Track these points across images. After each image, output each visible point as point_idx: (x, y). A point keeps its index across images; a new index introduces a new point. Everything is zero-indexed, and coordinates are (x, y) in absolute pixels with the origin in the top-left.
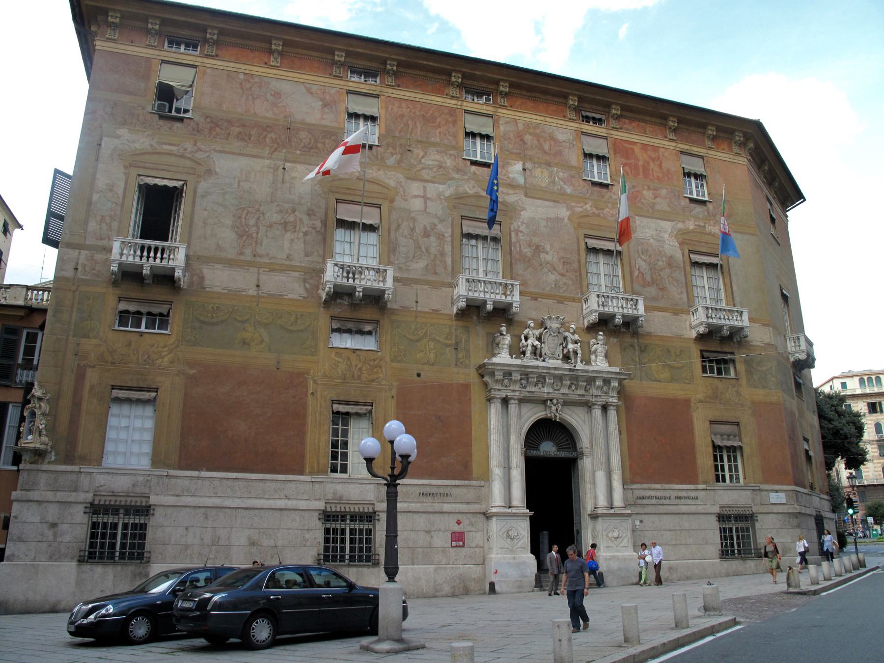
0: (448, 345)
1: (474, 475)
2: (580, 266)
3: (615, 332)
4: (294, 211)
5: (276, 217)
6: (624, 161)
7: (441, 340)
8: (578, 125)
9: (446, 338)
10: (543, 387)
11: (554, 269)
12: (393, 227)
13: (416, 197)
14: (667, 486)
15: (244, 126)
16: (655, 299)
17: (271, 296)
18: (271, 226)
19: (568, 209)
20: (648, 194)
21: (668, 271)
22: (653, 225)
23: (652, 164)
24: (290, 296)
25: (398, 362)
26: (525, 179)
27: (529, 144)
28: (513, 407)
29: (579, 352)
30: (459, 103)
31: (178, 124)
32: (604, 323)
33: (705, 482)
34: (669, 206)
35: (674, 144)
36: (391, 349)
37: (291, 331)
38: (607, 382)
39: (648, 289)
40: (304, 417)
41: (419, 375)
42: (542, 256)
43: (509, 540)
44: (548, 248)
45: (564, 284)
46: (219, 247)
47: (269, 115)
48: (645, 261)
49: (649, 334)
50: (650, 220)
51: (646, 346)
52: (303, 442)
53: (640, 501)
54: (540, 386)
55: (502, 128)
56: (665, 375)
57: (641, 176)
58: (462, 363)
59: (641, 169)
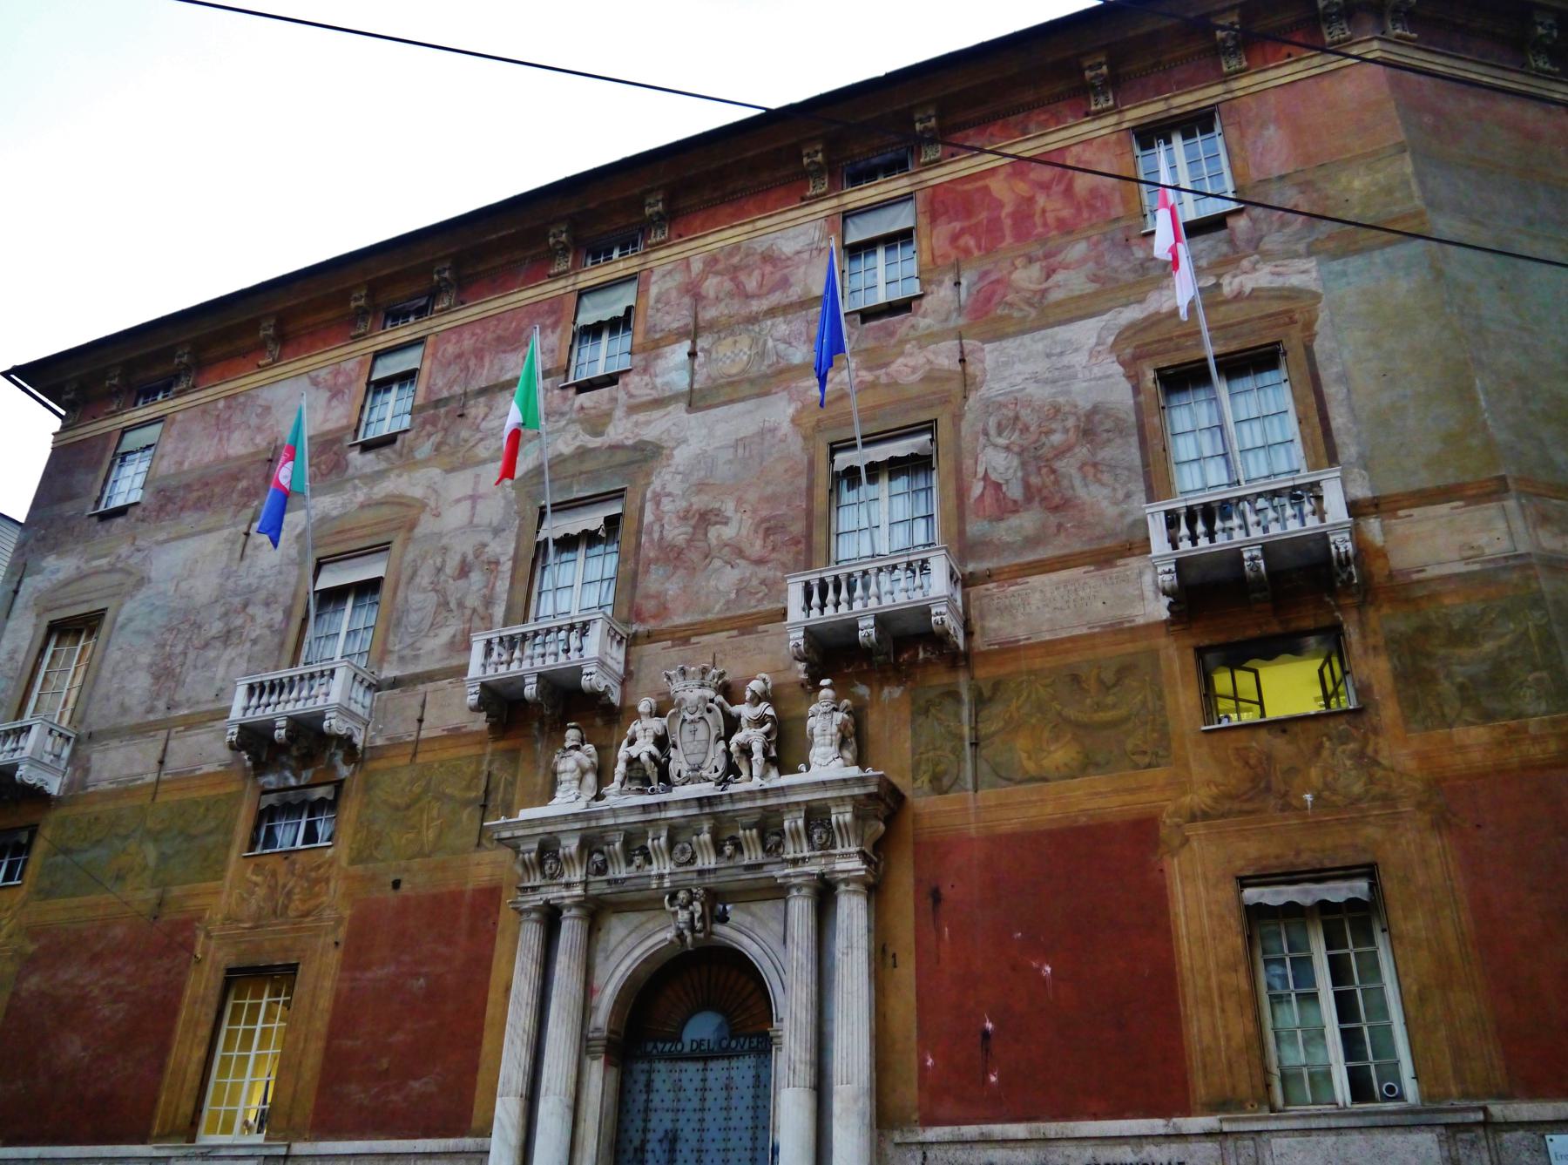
2: (810, 527)
3: (896, 667)
4: (245, 606)
5: (216, 627)
6: (957, 225)
7: (457, 793)
8: (834, 202)
9: (468, 788)
10: (651, 863)
11: (740, 553)
12: (404, 579)
13: (458, 501)
14: (1052, 1128)
15: (207, 484)
16: (1033, 542)
17: (178, 776)
18: (206, 645)
19: (791, 400)
20: (1026, 277)
21: (1082, 452)
22: (1040, 346)
23: (1041, 200)
24: (206, 769)
25: (361, 861)
26: (693, 373)
27: (712, 294)
28: (571, 931)
29: (757, 747)
30: (571, 281)
31: (120, 520)
32: (832, 654)
33: (1217, 1106)
34: (1095, 279)
35: (1113, 120)
36: (355, 834)
37: (195, 837)
38: (816, 816)
39: (1014, 521)
40: (174, 1013)
41: (396, 884)
42: (713, 532)
44: (729, 508)
45: (763, 582)
46: (124, 709)
47: (251, 449)
48: (1007, 448)
49: (1010, 649)
50: (1027, 338)
51: (997, 685)
52: (160, 1068)
54: (638, 860)
55: (654, 291)
56: (1061, 755)
57: (1009, 240)
59: (1008, 222)
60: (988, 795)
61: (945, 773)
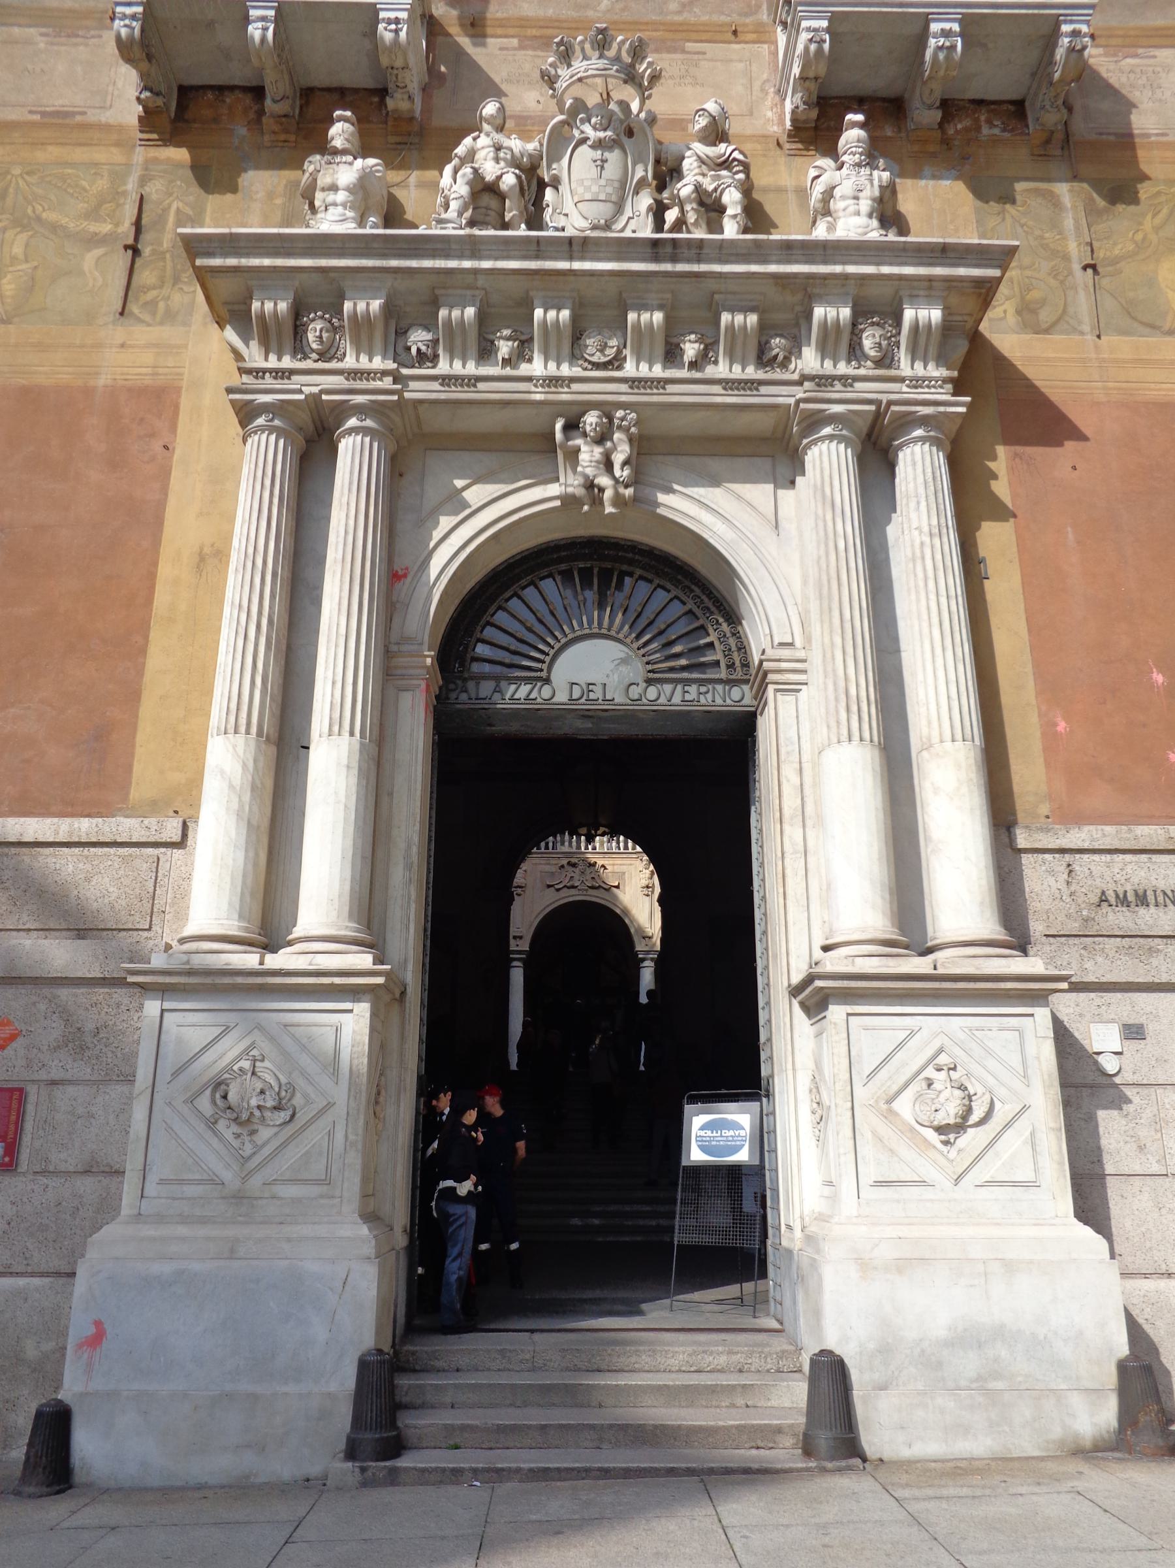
0: (94, 241)
1: (134, 794)
9: (93, 214)
29: (732, 198)
43: (226, 1129)
53: (1118, 919)
58: (151, 306)
60: (1118, 345)
61: (1043, 302)
